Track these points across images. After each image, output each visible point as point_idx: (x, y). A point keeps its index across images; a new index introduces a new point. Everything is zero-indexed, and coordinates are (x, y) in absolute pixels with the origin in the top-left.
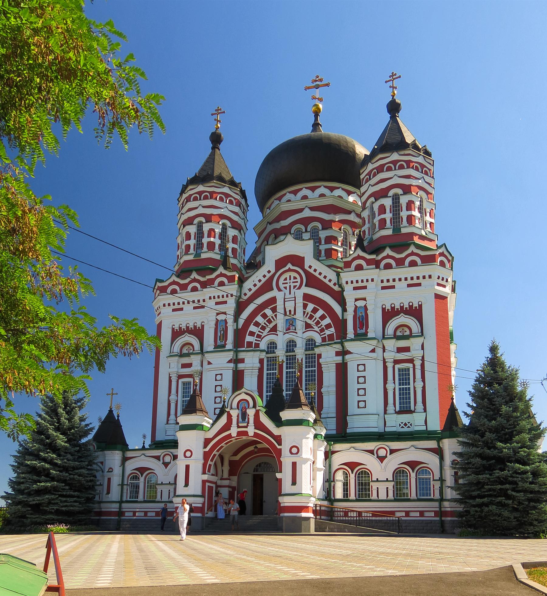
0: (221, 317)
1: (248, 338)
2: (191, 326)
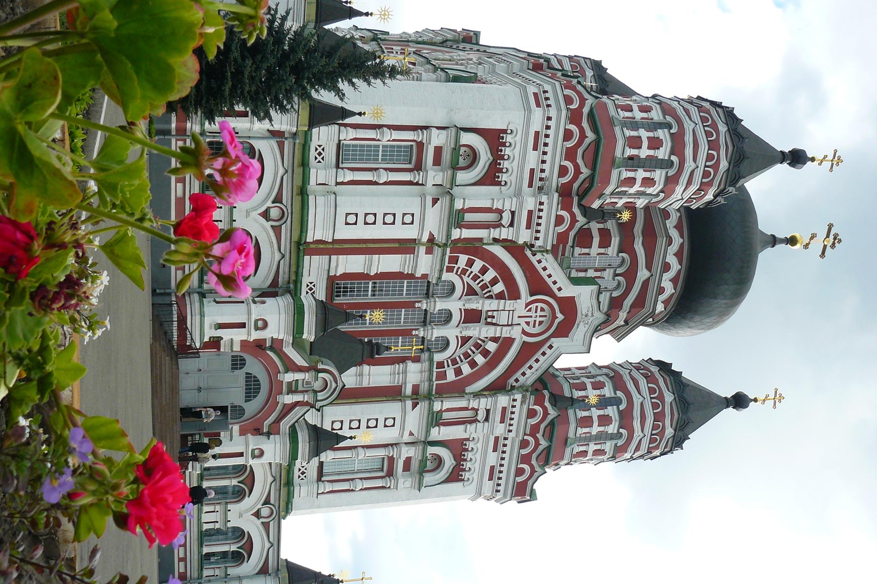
0: (506, 218)
1: (463, 259)
2: (505, 164)
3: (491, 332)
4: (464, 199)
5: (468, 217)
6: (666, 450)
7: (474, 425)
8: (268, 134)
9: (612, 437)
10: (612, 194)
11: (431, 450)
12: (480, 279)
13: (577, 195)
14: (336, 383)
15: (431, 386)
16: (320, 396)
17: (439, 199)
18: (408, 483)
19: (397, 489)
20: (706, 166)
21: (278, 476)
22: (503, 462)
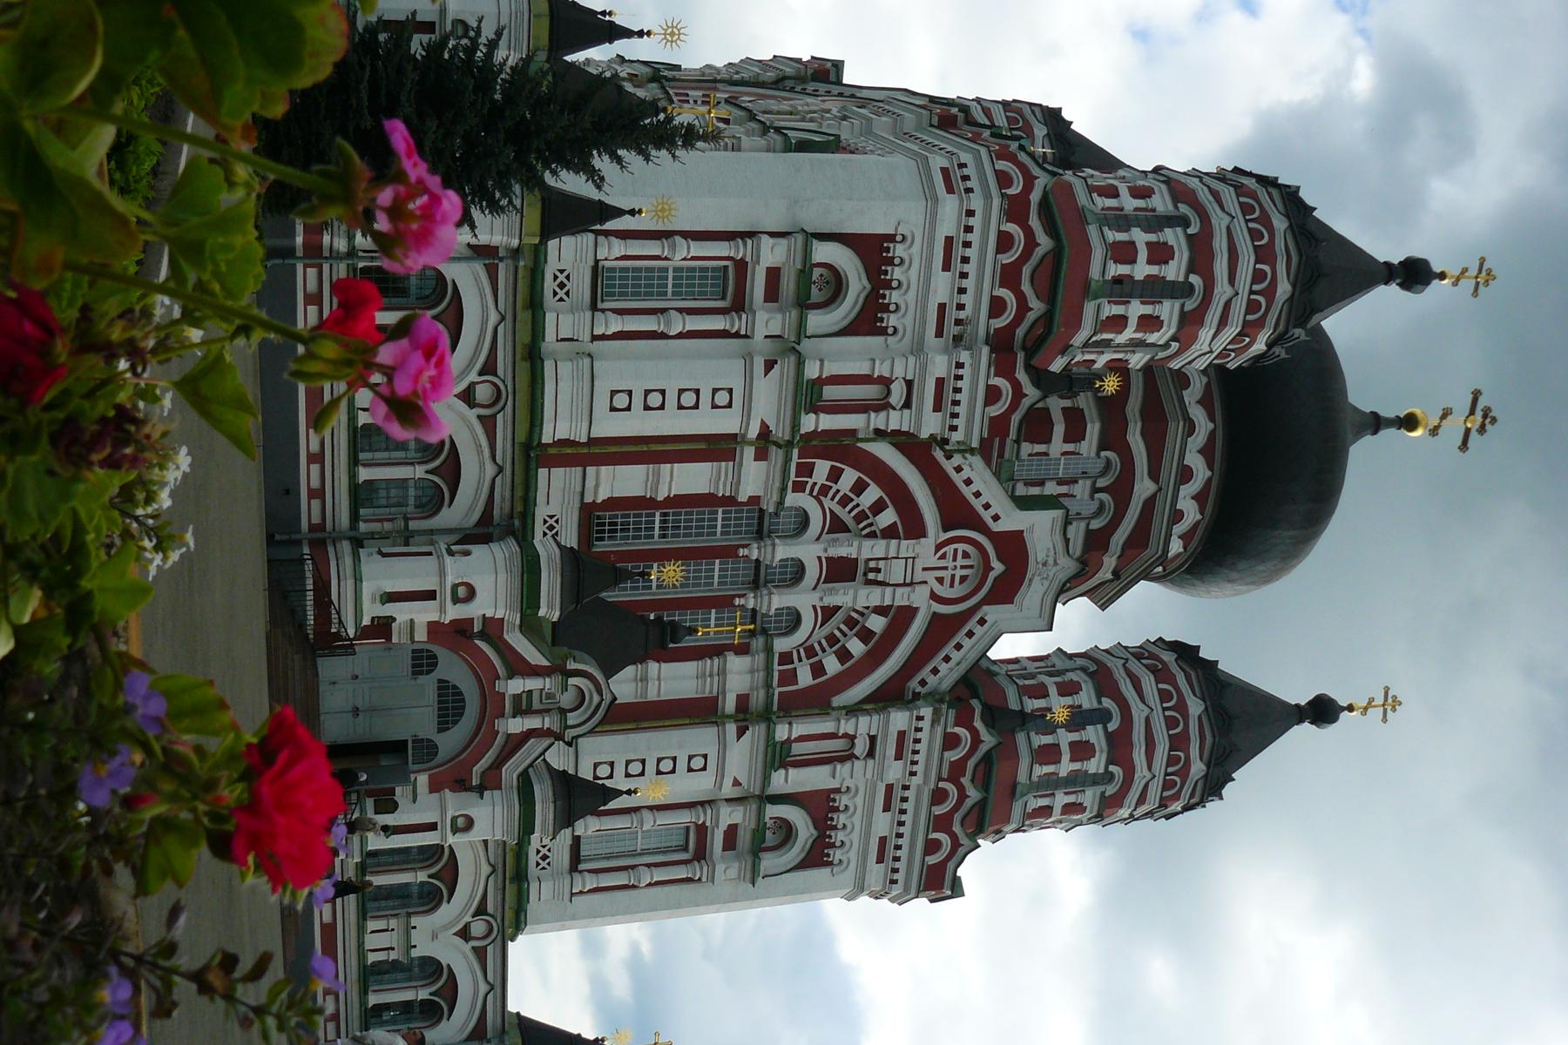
0: (897, 396)
1: (822, 468)
2: (894, 297)
3: (874, 597)
4: (822, 361)
5: (831, 392)
6: (1192, 801)
7: (848, 765)
8: (468, 252)
9: (1095, 780)
10: (1086, 345)
11: (773, 811)
12: (854, 503)
13: (1024, 348)
14: (600, 693)
15: (769, 697)
16: (572, 719)
17: (776, 362)
18: (733, 872)
19: (713, 882)
20: (1252, 292)
21: (500, 865)
22: (902, 830)
